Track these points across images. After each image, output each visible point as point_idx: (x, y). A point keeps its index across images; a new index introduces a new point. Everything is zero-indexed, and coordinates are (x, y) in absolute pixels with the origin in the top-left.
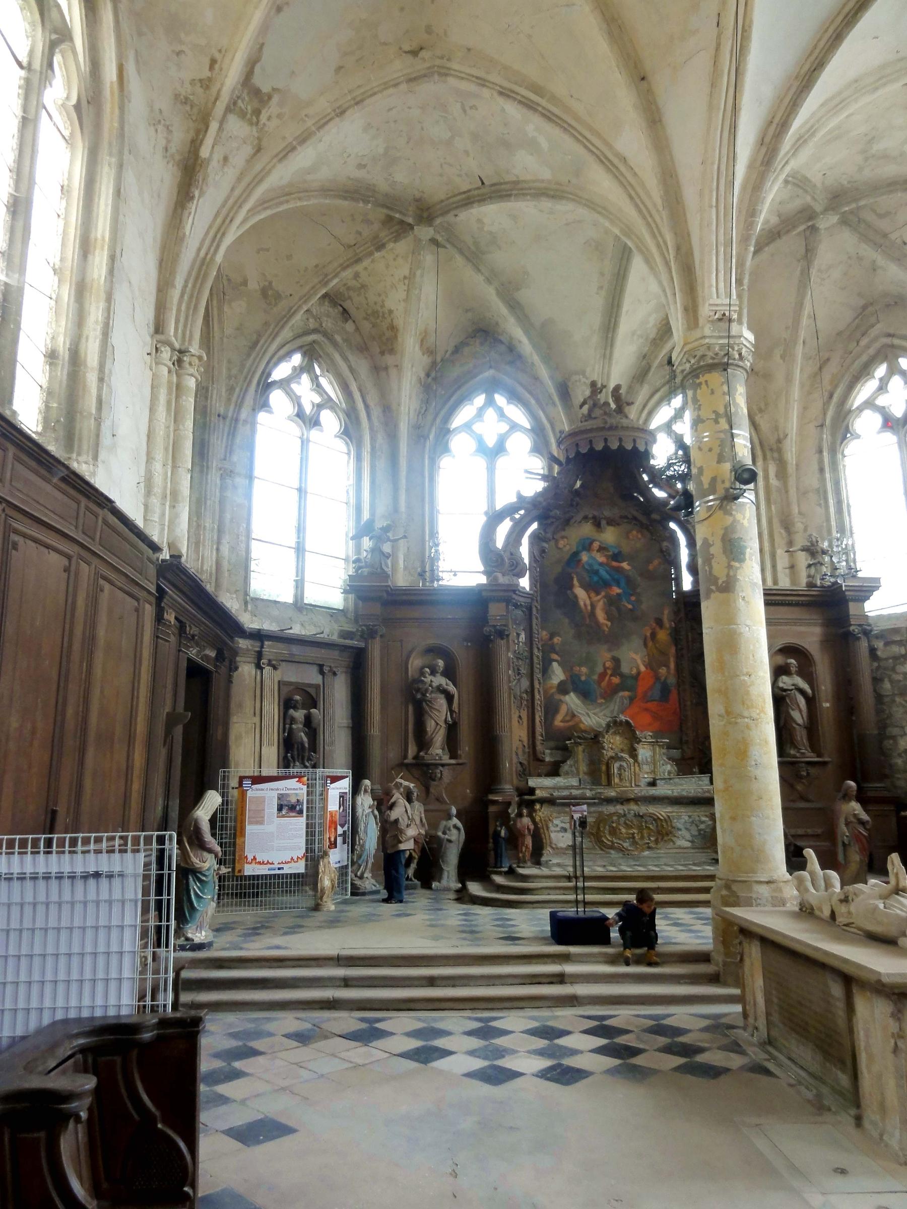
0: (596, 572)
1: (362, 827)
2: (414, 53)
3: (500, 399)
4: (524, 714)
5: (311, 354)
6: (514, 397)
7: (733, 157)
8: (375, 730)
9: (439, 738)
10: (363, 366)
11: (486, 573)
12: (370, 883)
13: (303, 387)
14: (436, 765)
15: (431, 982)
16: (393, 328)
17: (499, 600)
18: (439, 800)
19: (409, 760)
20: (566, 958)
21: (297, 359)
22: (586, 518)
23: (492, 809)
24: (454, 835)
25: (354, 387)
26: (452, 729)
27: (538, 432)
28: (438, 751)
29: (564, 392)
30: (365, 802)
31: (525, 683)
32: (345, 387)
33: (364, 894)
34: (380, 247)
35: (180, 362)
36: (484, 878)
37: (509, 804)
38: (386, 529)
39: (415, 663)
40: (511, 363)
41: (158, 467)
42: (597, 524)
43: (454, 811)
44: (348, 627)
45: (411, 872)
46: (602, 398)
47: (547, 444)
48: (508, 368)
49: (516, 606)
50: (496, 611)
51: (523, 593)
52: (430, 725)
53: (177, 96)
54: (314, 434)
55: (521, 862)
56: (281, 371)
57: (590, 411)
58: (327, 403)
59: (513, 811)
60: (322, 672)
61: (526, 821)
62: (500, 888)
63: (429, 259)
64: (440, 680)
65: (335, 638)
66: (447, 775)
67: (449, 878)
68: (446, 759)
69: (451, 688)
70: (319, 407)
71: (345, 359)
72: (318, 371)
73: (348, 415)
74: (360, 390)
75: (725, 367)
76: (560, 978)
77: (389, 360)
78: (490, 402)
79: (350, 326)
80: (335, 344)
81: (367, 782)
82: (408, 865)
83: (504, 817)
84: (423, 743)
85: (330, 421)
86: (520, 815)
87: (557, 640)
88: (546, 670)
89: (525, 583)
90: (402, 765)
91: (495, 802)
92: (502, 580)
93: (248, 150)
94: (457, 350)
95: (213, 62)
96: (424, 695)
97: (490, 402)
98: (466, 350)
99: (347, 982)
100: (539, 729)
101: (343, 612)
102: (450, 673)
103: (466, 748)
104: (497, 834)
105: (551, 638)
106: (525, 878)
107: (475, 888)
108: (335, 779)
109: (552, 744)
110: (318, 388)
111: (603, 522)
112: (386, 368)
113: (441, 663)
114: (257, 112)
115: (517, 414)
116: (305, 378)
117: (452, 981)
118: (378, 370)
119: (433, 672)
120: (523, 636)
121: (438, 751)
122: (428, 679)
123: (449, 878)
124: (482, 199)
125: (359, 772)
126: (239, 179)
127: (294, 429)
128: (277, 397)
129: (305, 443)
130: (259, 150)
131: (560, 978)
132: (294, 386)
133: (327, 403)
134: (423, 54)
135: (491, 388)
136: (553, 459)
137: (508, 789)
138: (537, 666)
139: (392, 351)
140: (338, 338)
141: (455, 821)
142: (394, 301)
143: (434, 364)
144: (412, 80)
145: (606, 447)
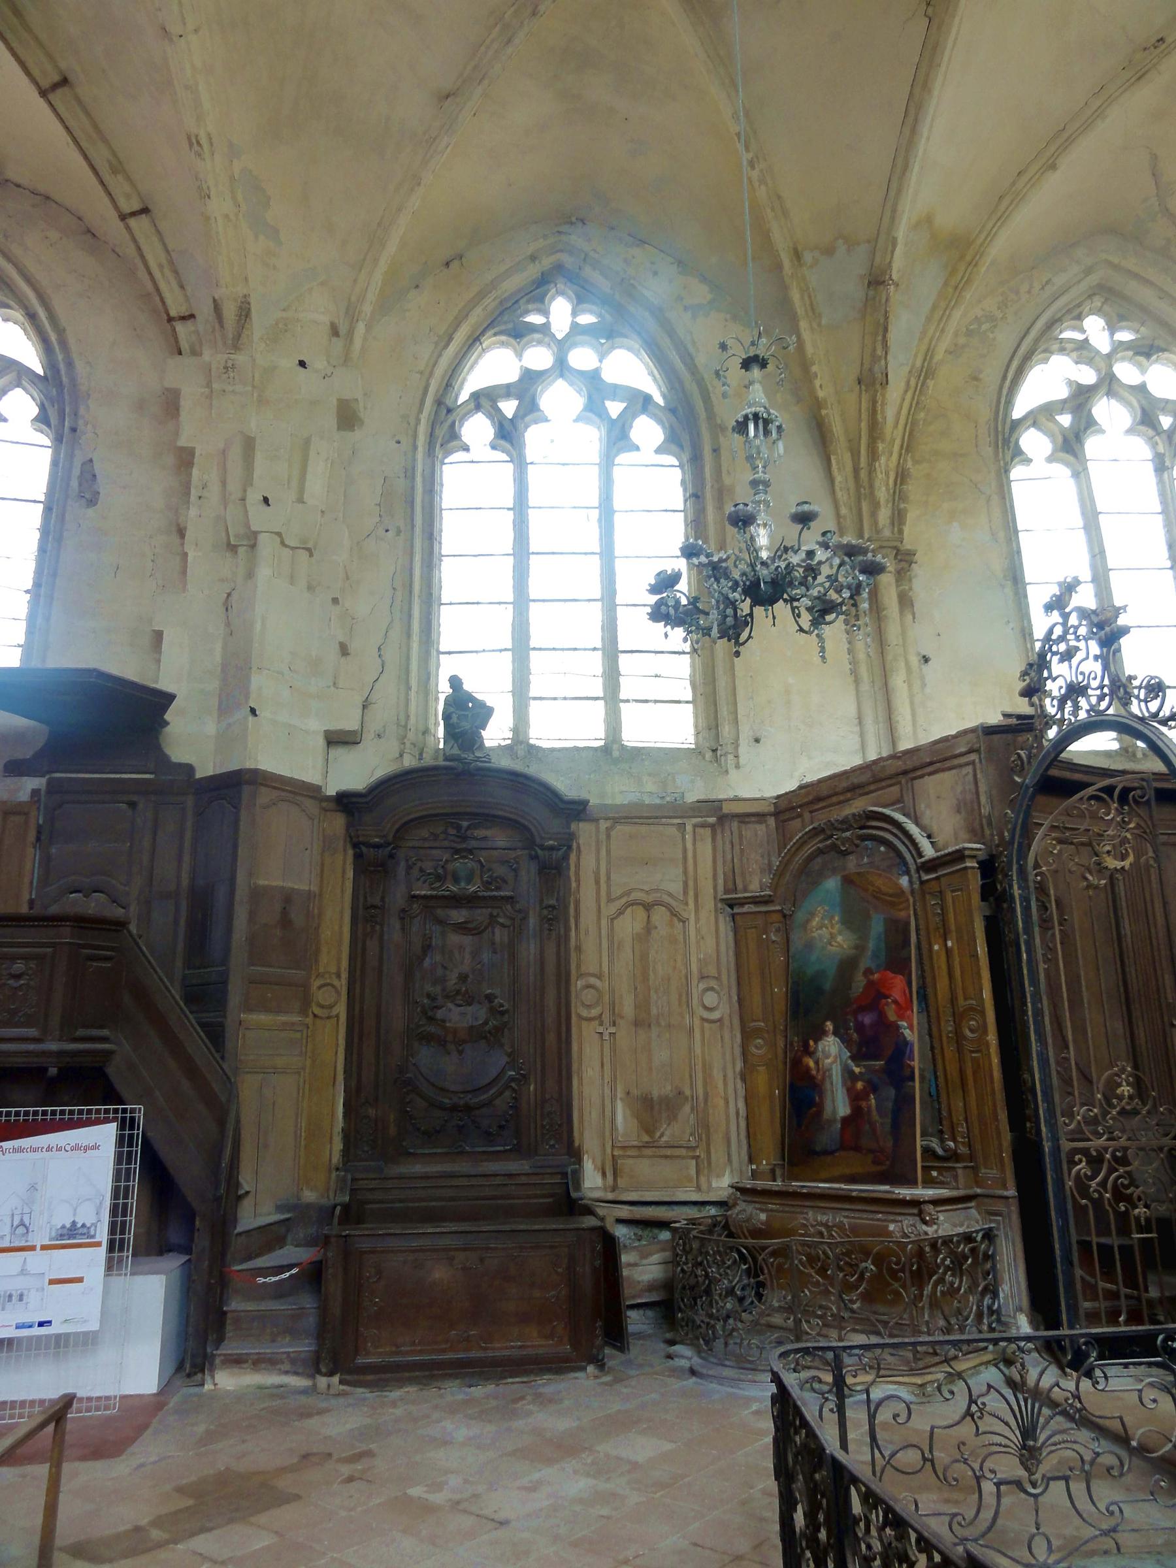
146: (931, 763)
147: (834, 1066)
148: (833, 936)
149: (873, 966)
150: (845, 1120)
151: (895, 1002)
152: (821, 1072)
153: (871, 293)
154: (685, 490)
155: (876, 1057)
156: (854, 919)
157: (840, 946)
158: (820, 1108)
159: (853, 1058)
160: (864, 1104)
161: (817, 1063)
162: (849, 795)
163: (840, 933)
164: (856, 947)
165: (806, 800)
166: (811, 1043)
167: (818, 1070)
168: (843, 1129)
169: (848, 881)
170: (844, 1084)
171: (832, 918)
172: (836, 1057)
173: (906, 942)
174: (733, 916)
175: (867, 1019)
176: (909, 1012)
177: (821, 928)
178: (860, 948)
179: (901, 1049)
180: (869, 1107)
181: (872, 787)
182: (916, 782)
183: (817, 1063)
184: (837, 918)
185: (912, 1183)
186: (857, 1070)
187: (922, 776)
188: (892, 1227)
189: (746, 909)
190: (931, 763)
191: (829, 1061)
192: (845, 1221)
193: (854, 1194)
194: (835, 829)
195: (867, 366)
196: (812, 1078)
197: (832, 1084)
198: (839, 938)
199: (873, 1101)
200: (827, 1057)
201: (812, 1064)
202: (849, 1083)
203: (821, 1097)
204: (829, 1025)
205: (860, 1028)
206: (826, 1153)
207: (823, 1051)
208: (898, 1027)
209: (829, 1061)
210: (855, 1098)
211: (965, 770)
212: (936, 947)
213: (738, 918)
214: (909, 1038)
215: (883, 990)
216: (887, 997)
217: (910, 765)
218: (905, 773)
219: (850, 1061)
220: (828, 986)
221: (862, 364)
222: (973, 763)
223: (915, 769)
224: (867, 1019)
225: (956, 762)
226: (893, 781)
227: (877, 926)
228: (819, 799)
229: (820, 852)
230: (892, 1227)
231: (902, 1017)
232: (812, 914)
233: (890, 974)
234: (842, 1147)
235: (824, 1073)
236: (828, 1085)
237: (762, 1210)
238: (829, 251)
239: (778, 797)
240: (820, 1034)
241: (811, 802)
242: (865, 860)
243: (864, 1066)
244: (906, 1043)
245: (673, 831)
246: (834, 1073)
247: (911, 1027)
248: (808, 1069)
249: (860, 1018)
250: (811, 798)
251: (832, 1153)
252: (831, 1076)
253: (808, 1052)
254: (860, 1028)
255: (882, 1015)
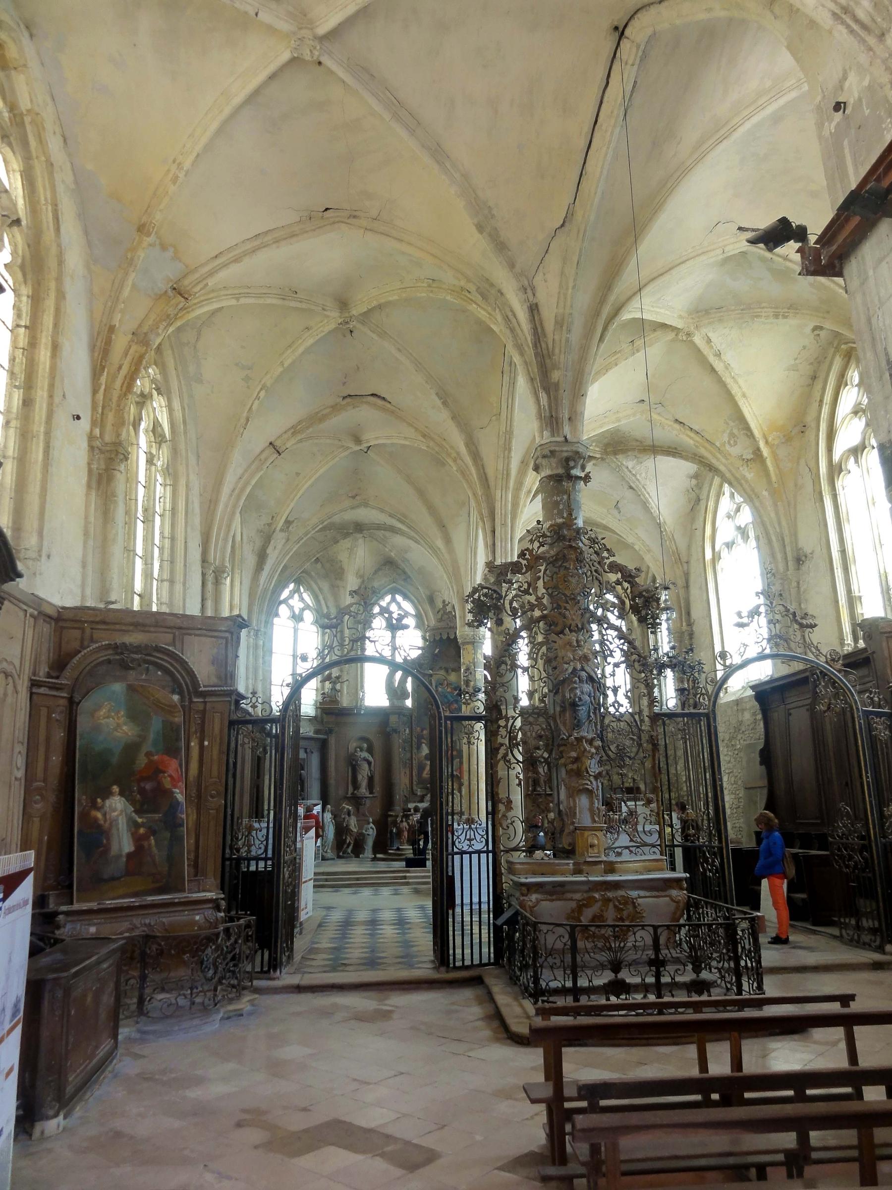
0: (446, 697)
1: (326, 828)
2: (354, 497)
3: (399, 598)
4: (408, 773)
5: (298, 582)
6: (406, 597)
7: (476, 563)
8: (332, 782)
9: (364, 784)
10: (325, 586)
11: (390, 699)
12: (330, 855)
13: (296, 603)
14: (362, 798)
15: (358, 879)
16: (342, 569)
17: (394, 713)
18: (364, 815)
19: (349, 795)
20: (408, 872)
21: (292, 586)
22: (441, 668)
23: (389, 819)
24: (371, 832)
25: (321, 597)
26: (371, 779)
27: (418, 617)
28: (363, 790)
29: (431, 600)
30: (328, 816)
31: (408, 755)
32: (316, 597)
33: (328, 860)
34: (336, 542)
35: (256, 635)
36: (385, 852)
37: (397, 816)
38: (338, 678)
39: (353, 745)
40: (405, 580)
41: (250, 681)
42: (447, 671)
43: (371, 820)
44: (318, 727)
45: (349, 850)
46: (449, 609)
47: (423, 624)
48: (403, 583)
49: (404, 715)
50: (393, 719)
51: (408, 708)
52: (360, 777)
53: (258, 530)
54: (301, 624)
55: (402, 844)
56: (285, 594)
57: (442, 615)
58: (307, 607)
59: (399, 820)
60: (306, 752)
61: (405, 824)
62: (391, 854)
63: (361, 541)
64: (365, 755)
65: (311, 734)
66: (368, 803)
67: (368, 853)
68: (368, 795)
69: (371, 759)
70: (303, 610)
71: (317, 584)
72: (302, 590)
73: (317, 611)
74: (324, 599)
75: (473, 643)
76: (405, 878)
77: (338, 582)
78: (393, 600)
79: (319, 566)
80: (311, 577)
81: (329, 806)
82: (348, 847)
83: (395, 823)
84: (356, 785)
85: (309, 616)
86: (402, 821)
87: (425, 732)
88: (419, 748)
89: (409, 703)
90: (346, 798)
91: (391, 816)
92: (396, 703)
93: (284, 541)
94: (376, 572)
95: (273, 517)
96: (356, 762)
97: (393, 600)
98: (380, 573)
99: (326, 880)
100: (415, 778)
101: (315, 718)
102: (370, 750)
103: (377, 789)
104: (392, 831)
105: (422, 731)
106: (403, 850)
107: (379, 856)
108: (316, 805)
109: (421, 786)
110: (302, 599)
111: (450, 671)
112: (338, 587)
113: (365, 745)
114: (288, 528)
115: (408, 606)
116: (296, 596)
117: (365, 879)
118: (334, 588)
119: (361, 750)
120: (407, 730)
121: (363, 790)
122: (359, 754)
123: (368, 853)
124: (385, 530)
125: (325, 801)
126: (280, 554)
127: (291, 623)
128: (283, 610)
129: (296, 630)
130: (288, 540)
131: (405, 878)
132: (291, 602)
133: (307, 607)
134: (358, 498)
135: (394, 592)
136: (424, 638)
137: (398, 809)
138: (415, 746)
139: (341, 579)
140: (313, 574)
141: (371, 825)
142: (343, 557)
143: (363, 582)
144: (352, 508)
145: (448, 637)
146: (200, 629)
147: (120, 818)
148: (118, 725)
149: (153, 750)
150: (129, 855)
151: (171, 776)
152: (108, 822)
153: (170, 293)
154: (18, 315)
155: (155, 811)
156: (134, 716)
157: (126, 733)
158: (107, 849)
159: (136, 812)
160: (146, 844)
161: (105, 815)
162: (131, 628)
163: (125, 724)
164: (139, 736)
165: (91, 619)
166: (99, 800)
167: (105, 821)
168: (127, 861)
169: (131, 688)
170: (129, 830)
171: (118, 712)
172: (122, 811)
173: (178, 739)
174: (32, 694)
175: (148, 786)
176: (180, 783)
177: (108, 717)
178: (143, 738)
179: (174, 805)
180: (150, 845)
181: (152, 629)
182: (186, 638)
183: (105, 815)
184: (122, 713)
185: (184, 891)
186: (140, 820)
187: (190, 635)
188: (197, 918)
189: (42, 690)
190: (200, 629)
191: (116, 814)
192: (164, 920)
193: (176, 901)
194: (128, 650)
195: (145, 328)
196: (99, 826)
197: (118, 830)
198: (125, 728)
199: (153, 842)
200: (114, 811)
201: (99, 815)
202: (133, 829)
203: (108, 839)
204: (116, 789)
205: (142, 791)
206: (113, 879)
207: (110, 806)
208: (173, 793)
209: (116, 814)
210: (138, 840)
211: (220, 641)
212: (192, 744)
213: (35, 697)
214: (180, 800)
215: (160, 767)
216: (164, 772)
217: (185, 625)
218: (180, 628)
219: (133, 814)
220: (115, 760)
221: (140, 326)
222: (227, 639)
223: (188, 629)
224: (148, 786)
225: (216, 634)
226: (169, 630)
227: (156, 724)
228: (104, 622)
229: (109, 662)
230: (197, 918)
231: (175, 786)
232: (100, 707)
233: (166, 758)
234: (129, 873)
235: (111, 824)
236: (114, 831)
237: (89, 925)
238: (164, 247)
239: (63, 608)
240: (107, 794)
241: (97, 623)
242: (144, 677)
243: (146, 818)
244: (178, 803)
245: (21, 614)
246: (120, 821)
247: (181, 793)
248: (96, 819)
249: (142, 785)
250: (97, 619)
251: (118, 878)
252: (117, 824)
253: (94, 806)
254: (142, 791)
255: (159, 783)
